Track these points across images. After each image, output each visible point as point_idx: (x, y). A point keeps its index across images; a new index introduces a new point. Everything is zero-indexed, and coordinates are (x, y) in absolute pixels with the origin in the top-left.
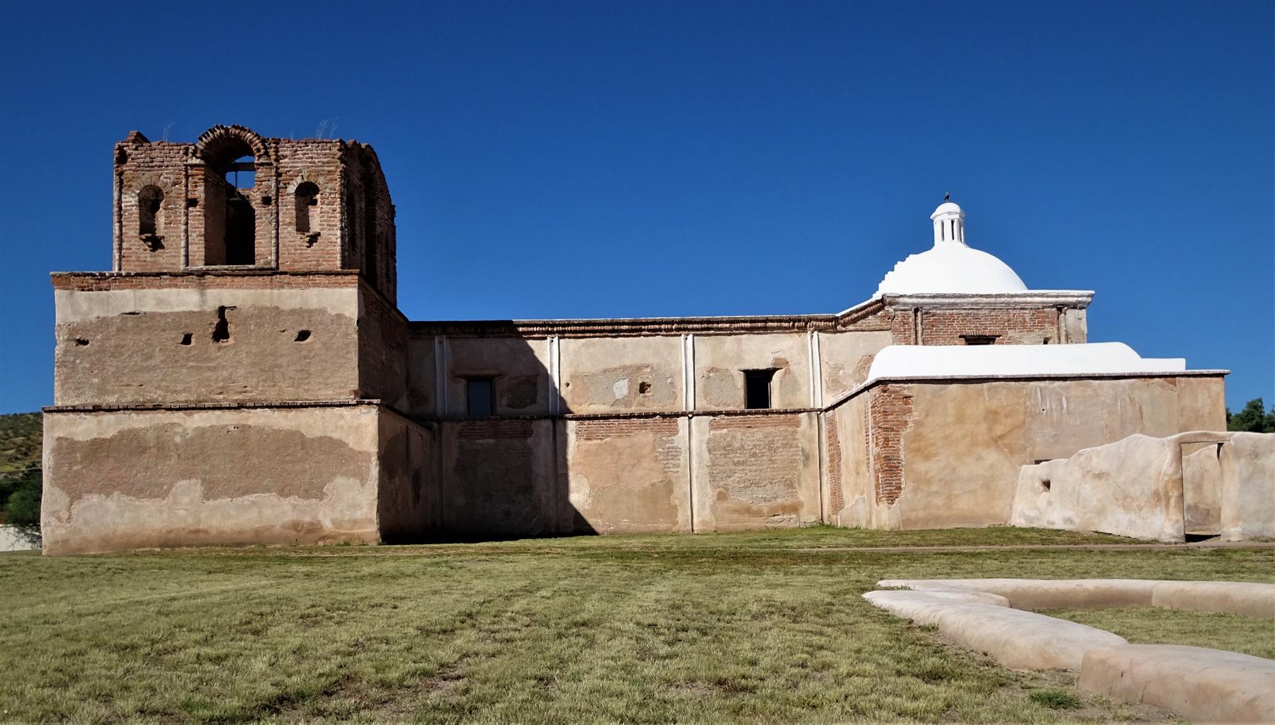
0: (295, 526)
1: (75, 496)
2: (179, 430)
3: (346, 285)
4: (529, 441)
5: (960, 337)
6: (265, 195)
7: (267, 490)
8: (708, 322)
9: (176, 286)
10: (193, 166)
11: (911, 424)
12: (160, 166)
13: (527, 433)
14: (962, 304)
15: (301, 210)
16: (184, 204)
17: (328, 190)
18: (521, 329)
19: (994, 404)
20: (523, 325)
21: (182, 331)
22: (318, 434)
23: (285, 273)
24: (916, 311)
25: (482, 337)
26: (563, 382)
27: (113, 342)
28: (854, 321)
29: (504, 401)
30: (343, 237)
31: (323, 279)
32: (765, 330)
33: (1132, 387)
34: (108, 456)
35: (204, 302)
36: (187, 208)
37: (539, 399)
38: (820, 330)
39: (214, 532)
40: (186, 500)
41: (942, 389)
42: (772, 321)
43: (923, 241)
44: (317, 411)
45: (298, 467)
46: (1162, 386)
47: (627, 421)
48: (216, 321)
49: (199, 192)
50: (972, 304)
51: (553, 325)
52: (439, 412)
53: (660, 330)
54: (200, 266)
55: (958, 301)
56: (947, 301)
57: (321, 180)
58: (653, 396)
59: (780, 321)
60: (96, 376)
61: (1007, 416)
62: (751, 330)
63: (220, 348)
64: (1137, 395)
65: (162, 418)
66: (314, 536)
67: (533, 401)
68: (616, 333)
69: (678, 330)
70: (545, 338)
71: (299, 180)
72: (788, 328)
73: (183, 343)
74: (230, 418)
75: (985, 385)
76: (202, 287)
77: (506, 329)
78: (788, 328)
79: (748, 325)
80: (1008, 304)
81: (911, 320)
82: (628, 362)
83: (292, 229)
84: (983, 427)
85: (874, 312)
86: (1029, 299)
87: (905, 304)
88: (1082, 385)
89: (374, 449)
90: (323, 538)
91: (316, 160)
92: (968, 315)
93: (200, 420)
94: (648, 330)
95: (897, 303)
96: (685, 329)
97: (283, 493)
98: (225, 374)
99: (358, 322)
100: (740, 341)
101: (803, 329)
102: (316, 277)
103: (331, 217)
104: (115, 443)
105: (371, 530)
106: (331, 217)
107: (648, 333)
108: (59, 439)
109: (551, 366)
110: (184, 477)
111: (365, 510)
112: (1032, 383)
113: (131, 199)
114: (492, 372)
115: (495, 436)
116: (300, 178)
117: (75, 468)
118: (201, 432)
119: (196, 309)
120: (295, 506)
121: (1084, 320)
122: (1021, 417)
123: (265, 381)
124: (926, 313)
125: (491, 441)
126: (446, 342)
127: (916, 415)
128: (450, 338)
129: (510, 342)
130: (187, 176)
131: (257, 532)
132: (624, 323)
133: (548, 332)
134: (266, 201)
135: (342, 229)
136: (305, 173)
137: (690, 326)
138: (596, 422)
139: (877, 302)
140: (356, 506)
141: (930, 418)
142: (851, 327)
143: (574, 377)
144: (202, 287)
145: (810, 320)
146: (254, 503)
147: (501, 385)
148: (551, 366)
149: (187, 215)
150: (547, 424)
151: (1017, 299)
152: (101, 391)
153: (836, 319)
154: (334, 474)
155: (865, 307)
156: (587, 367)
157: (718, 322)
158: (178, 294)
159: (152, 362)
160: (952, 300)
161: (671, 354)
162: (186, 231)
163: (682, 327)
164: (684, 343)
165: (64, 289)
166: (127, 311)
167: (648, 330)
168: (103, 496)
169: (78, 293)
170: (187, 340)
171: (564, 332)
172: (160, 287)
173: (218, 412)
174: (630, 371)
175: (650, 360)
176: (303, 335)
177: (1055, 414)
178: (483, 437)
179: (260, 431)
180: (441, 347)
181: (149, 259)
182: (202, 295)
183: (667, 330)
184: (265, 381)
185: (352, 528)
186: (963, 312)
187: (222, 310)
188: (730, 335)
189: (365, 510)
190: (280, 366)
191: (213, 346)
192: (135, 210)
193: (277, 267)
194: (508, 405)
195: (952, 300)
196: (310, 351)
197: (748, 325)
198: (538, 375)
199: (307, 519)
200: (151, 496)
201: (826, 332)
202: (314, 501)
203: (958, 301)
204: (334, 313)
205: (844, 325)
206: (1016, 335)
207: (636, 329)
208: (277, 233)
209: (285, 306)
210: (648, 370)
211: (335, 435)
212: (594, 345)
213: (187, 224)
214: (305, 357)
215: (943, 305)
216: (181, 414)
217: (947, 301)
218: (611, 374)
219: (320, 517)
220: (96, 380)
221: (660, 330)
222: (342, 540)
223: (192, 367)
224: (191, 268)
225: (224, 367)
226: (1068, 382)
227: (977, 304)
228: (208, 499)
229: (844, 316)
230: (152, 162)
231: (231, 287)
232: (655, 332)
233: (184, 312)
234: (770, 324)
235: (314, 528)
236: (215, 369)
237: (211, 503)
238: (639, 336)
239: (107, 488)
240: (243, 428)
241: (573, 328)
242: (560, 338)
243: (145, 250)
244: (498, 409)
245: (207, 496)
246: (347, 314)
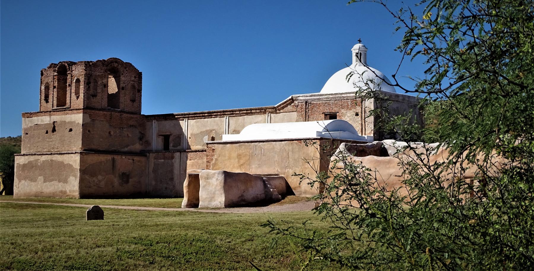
0: (61, 192)
1: (20, 181)
2: (39, 161)
3: (80, 113)
5: (323, 113)
7: (56, 180)
8: (232, 111)
9: (45, 115)
10: (55, 75)
11: (214, 160)
13: (173, 158)
14: (323, 98)
15: (78, 87)
16: (52, 88)
18: (176, 117)
19: (240, 152)
20: (177, 115)
22: (67, 163)
23: (73, 110)
24: (306, 102)
25: (166, 120)
26: (188, 137)
28: (283, 108)
30: (84, 96)
31: (75, 111)
32: (252, 114)
33: (286, 145)
36: (53, 89)
37: (181, 144)
38: (272, 113)
39: (45, 193)
40: (40, 183)
41: (225, 146)
42: (253, 110)
43: (348, 64)
44: (67, 155)
46: (296, 144)
47: (202, 153)
48: (53, 126)
49: (56, 84)
50: (326, 98)
51: (185, 115)
52: (153, 149)
53: (217, 115)
54: (55, 108)
55: (321, 97)
56: (316, 97)
57: (80, 78)
59: (256, 110)
61: (244, 157)
62: (247, 114)
64: (287, 148)
65: (37, 157)
66: (65, 195)
67: (180, 145)
68: (205, 117)
69: (224, 115)
70: (183, 120)
71: (76, 78)
72: (258, 113)
74: (49, 157)
75: (238, 144)
76: (50, 115)
77: (170, 117)
78: (258, 113)
79: (245, 112)
80: (340, 97)
81: (304, 107)
82: (208, 129)
83: (74, 94)
84: (237, 160)
85: (290, 104)
86: (348, 95)
87: (301, 100)
88: (269, 144)
89: (79, 168)
90: (67, 196)
92: (326, 103)
93: (44, 158)
94: (214, 115)
95: (297, 100)
96: (225, 115)
97: (59, 182)
98: (54, 143)
99: (83, 125)
100: (244, 119)
101: (265, 113)
102: (74, 111)
105: (77, 194)
107: (214, 116)
109: (185, 131)
110: (40, 176)
111: (76, 187)
112: (253, 144)
115: (164, 159)
118: (44, 161)
120: (61, 185)
121: (373, 103)
122: (248, 157)
124: (310, 103)
125: (163, 160)
127: (216, 157)
129: (174, 122)
130: (54, 79)
131: (54, 193)
132: (205, 113)
133: (184, 118)
134: (69, 85)
135: (84, 93)
137: (226, 113)
138: (193, 153)
139: (290, 99)
140: (74, 186)
141: (220, 157)
142: (281, 111)
143: (191, 135)
144: (50, 115)
145: (267, 108)
146: (53, 184)
147: (171, 139)
148: (185, 131)
149: (53, 91)
150: (177, 154)
151: (343, 95)
152: (30, 149)
153: (274, 108)
154: (70, 176)
155: (285, 102)
156: (196, 131)
157: (235, 111)
158: (46, 118)
160: (318, 97)
161: (221, 124)
162: (53, 97)
163: (223, 114)
164: (225, 119)
167: (214, 115)
169: (27, 119)
170: (47, 132)
171: (188, 117)
172: (42, 116)
173: (47, 156)
174: (209, 132)
175: (215, 128)
176: (71, 130)
177: (259, 156)
178: (161, 159)
179: (55, 161)
180: (155, 124)
182: (50, 118)
183: (220, 115)
185: (73, 193)
186: (324, 102)
187: (54, 122)
188: (241, 116)
189: (76, 187)
192: (44, 90)
193: (70, 108)
194: (173, 146)
195: (318, 97)
197: (245, 112)
198: (180, 136)
199: (64, 190)
200: (34, 181)
201: (274, 114)
202: (65, 184)
203: (321, 97)
204: (77, 122)
205: (279, 110)
206: (345, 112)
207: (210, 115)
208: (71, 96)
209: (67, 121)
210: (214, 131)
211: (71, 163)
212: (198, 122)
213: (53, 94)
214: (71, 137)
215: (315, 99)
216: (40, 156)
217: (316, 97)
218: (203, 134)
219: (67, 189)
221: (217, 115)
222: (71, 197)
224: (54, 108)
226: (265, 143)
227: (328, 98)
229: (278, 106)
231: (56, 115)
232: (216, 116)
234: (253, 111)
235: (65, 192)
236: (51, 141)
237: (45, 184)
238: (212, 118)
239: (25, 179)
240: (52, 160)
241: (191, 116)
242: (188, 120)
245: (45, 182)
246: (80, 123)
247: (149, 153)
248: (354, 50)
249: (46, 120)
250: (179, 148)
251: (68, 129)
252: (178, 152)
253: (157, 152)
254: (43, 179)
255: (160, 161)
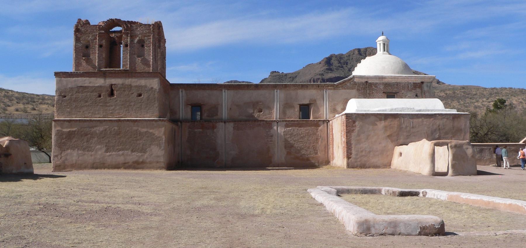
4: (215, 130)
6: (126, 44)
12: (89, 33)
13: (214, 127)
17: (148, 42)
21: (98, 93)
27: (74, 96)
29: (206, 115)
34: (74, 137)
35: (105, 82)
45: (138, 142)
58: (263, 113)
60: (68, 108)
63: (111, 99)
67: (217, 115)
73: (98, 97)
91: (144, 31)
98: (112, 108)
103: (149, 52)
104: (76, 132)
106: (149, 52)
108: (58, 130)
113: (79, 45)
114: (202, 103)
116: (138, 37)
117: (63, 141)
119: (103, 85)
123: (126, 111)
125: (201, 130)
126: (184, 91)
128: (186, 90)
136: (140, 36)
159: (87, 104)
165: (59, 78)
166: (79, 85)
168: (72, 151)
176: (140, 95)
181: (85, 66)
182: (105, 80)
184: (126, 111)
187: (112, 85)
190: (131, 106)
191: (108, 99)
196: (141, 101)
204: (150, 87)
209: (134, 84)
214: (140, 103)
220: (69, 110)
223: (101, 105)
225: (112, 106)
228: (107, 153)
230: (87, 31)
233: (99, 86)
236: (109, 106)
243: (84, 63)
244: (203, 117)
245: (107, 151)
247: (181, 123)
248: (379, 41)
249: (99, 82)
250: (215, 118)
251: (135, 94)
252: (222, 122)
253: (186, 121)
254: (104, 149)
255: (196, 130)
